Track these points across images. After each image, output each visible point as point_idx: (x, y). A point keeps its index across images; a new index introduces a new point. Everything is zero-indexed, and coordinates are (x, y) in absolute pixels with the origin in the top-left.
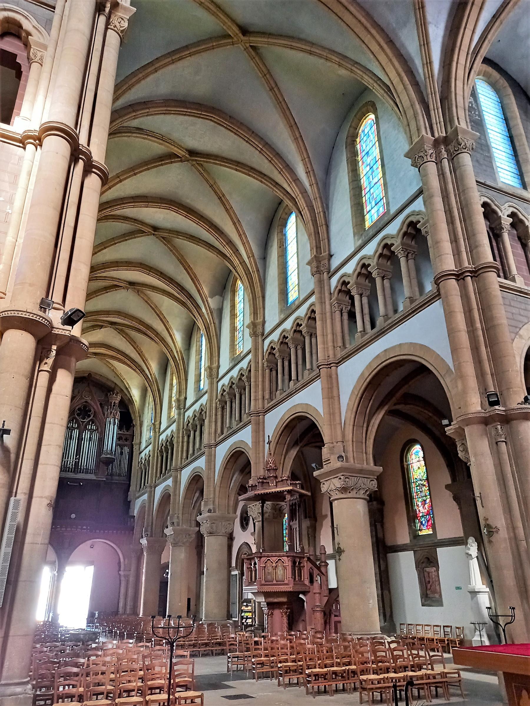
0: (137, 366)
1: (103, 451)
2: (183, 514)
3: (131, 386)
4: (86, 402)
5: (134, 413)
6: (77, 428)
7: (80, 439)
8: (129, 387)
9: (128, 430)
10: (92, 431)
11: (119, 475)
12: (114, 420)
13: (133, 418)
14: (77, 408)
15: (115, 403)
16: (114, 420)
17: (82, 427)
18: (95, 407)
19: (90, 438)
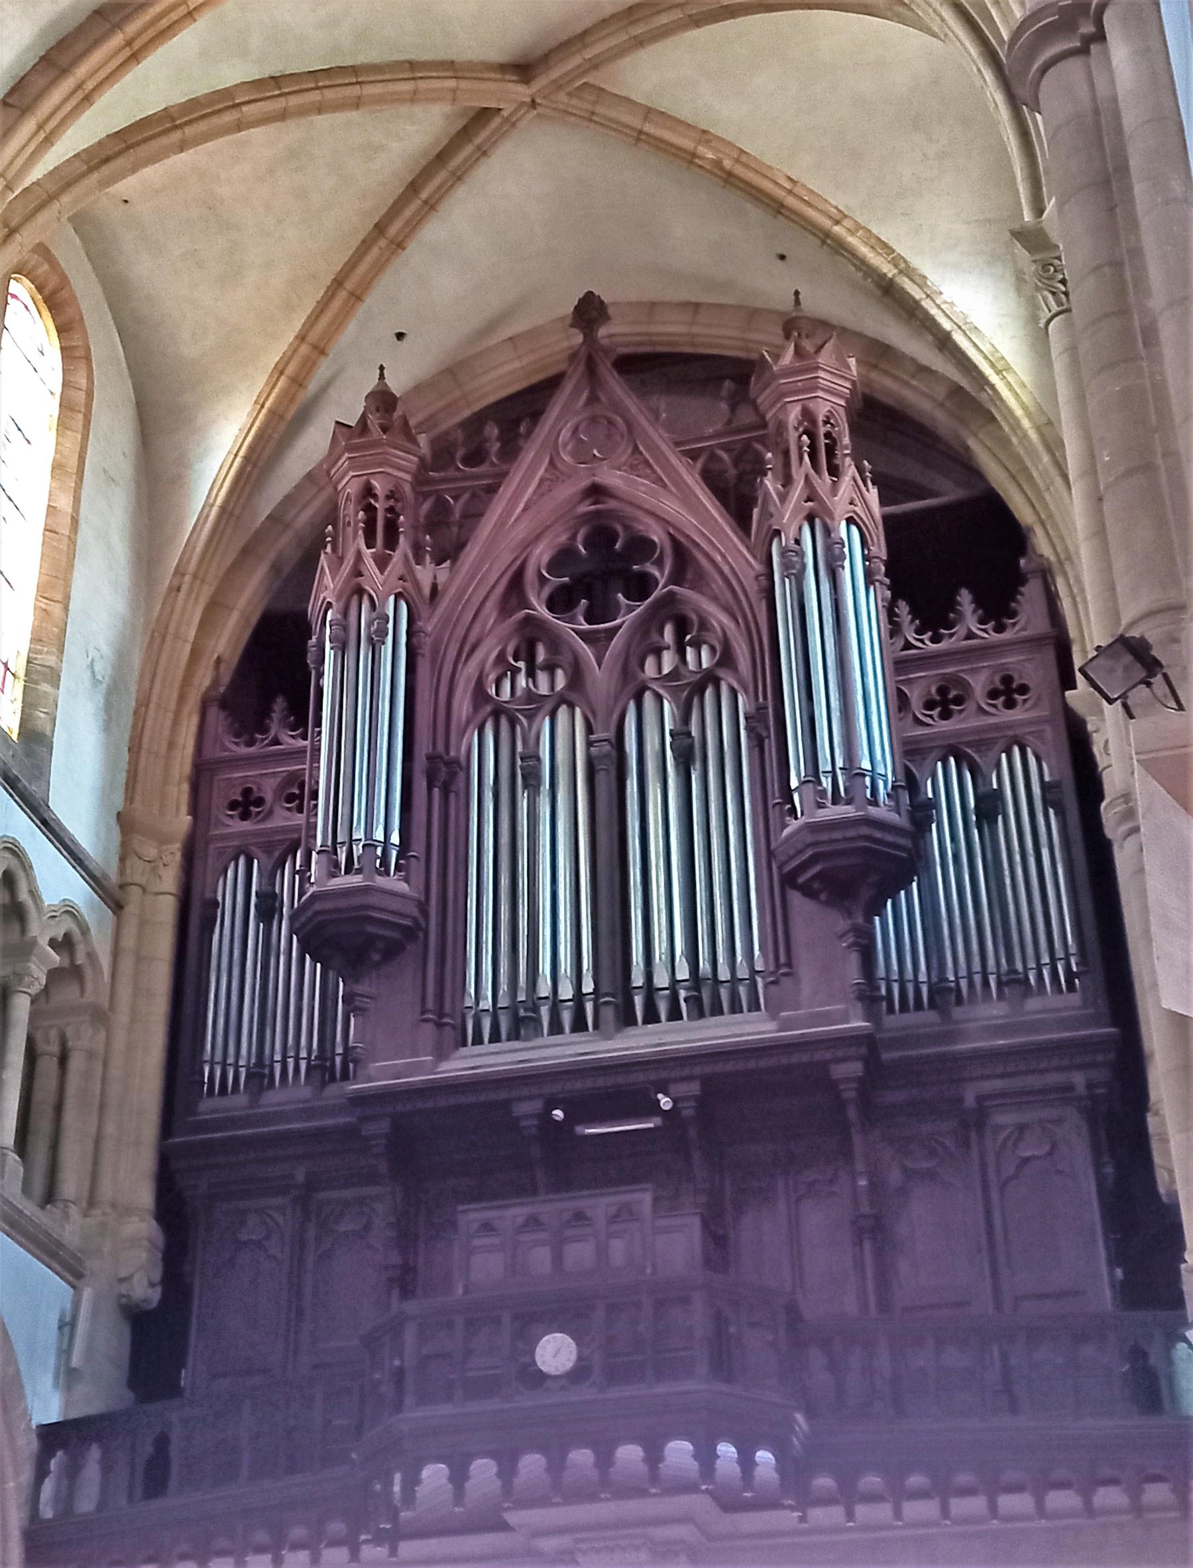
1: (787, 793)
3: (916, 262)
4: (596, 492)
5: (1020, 474)
7: (609, 771)
8: (908, 271)
9: (997, 609)
11: (1014, 983)
12: (827, 531)
13: (1024, 513)
14: (542, 554)
16: (827, 531)
17: (601, 676)
18: (671, 507)
19: (681, 734)
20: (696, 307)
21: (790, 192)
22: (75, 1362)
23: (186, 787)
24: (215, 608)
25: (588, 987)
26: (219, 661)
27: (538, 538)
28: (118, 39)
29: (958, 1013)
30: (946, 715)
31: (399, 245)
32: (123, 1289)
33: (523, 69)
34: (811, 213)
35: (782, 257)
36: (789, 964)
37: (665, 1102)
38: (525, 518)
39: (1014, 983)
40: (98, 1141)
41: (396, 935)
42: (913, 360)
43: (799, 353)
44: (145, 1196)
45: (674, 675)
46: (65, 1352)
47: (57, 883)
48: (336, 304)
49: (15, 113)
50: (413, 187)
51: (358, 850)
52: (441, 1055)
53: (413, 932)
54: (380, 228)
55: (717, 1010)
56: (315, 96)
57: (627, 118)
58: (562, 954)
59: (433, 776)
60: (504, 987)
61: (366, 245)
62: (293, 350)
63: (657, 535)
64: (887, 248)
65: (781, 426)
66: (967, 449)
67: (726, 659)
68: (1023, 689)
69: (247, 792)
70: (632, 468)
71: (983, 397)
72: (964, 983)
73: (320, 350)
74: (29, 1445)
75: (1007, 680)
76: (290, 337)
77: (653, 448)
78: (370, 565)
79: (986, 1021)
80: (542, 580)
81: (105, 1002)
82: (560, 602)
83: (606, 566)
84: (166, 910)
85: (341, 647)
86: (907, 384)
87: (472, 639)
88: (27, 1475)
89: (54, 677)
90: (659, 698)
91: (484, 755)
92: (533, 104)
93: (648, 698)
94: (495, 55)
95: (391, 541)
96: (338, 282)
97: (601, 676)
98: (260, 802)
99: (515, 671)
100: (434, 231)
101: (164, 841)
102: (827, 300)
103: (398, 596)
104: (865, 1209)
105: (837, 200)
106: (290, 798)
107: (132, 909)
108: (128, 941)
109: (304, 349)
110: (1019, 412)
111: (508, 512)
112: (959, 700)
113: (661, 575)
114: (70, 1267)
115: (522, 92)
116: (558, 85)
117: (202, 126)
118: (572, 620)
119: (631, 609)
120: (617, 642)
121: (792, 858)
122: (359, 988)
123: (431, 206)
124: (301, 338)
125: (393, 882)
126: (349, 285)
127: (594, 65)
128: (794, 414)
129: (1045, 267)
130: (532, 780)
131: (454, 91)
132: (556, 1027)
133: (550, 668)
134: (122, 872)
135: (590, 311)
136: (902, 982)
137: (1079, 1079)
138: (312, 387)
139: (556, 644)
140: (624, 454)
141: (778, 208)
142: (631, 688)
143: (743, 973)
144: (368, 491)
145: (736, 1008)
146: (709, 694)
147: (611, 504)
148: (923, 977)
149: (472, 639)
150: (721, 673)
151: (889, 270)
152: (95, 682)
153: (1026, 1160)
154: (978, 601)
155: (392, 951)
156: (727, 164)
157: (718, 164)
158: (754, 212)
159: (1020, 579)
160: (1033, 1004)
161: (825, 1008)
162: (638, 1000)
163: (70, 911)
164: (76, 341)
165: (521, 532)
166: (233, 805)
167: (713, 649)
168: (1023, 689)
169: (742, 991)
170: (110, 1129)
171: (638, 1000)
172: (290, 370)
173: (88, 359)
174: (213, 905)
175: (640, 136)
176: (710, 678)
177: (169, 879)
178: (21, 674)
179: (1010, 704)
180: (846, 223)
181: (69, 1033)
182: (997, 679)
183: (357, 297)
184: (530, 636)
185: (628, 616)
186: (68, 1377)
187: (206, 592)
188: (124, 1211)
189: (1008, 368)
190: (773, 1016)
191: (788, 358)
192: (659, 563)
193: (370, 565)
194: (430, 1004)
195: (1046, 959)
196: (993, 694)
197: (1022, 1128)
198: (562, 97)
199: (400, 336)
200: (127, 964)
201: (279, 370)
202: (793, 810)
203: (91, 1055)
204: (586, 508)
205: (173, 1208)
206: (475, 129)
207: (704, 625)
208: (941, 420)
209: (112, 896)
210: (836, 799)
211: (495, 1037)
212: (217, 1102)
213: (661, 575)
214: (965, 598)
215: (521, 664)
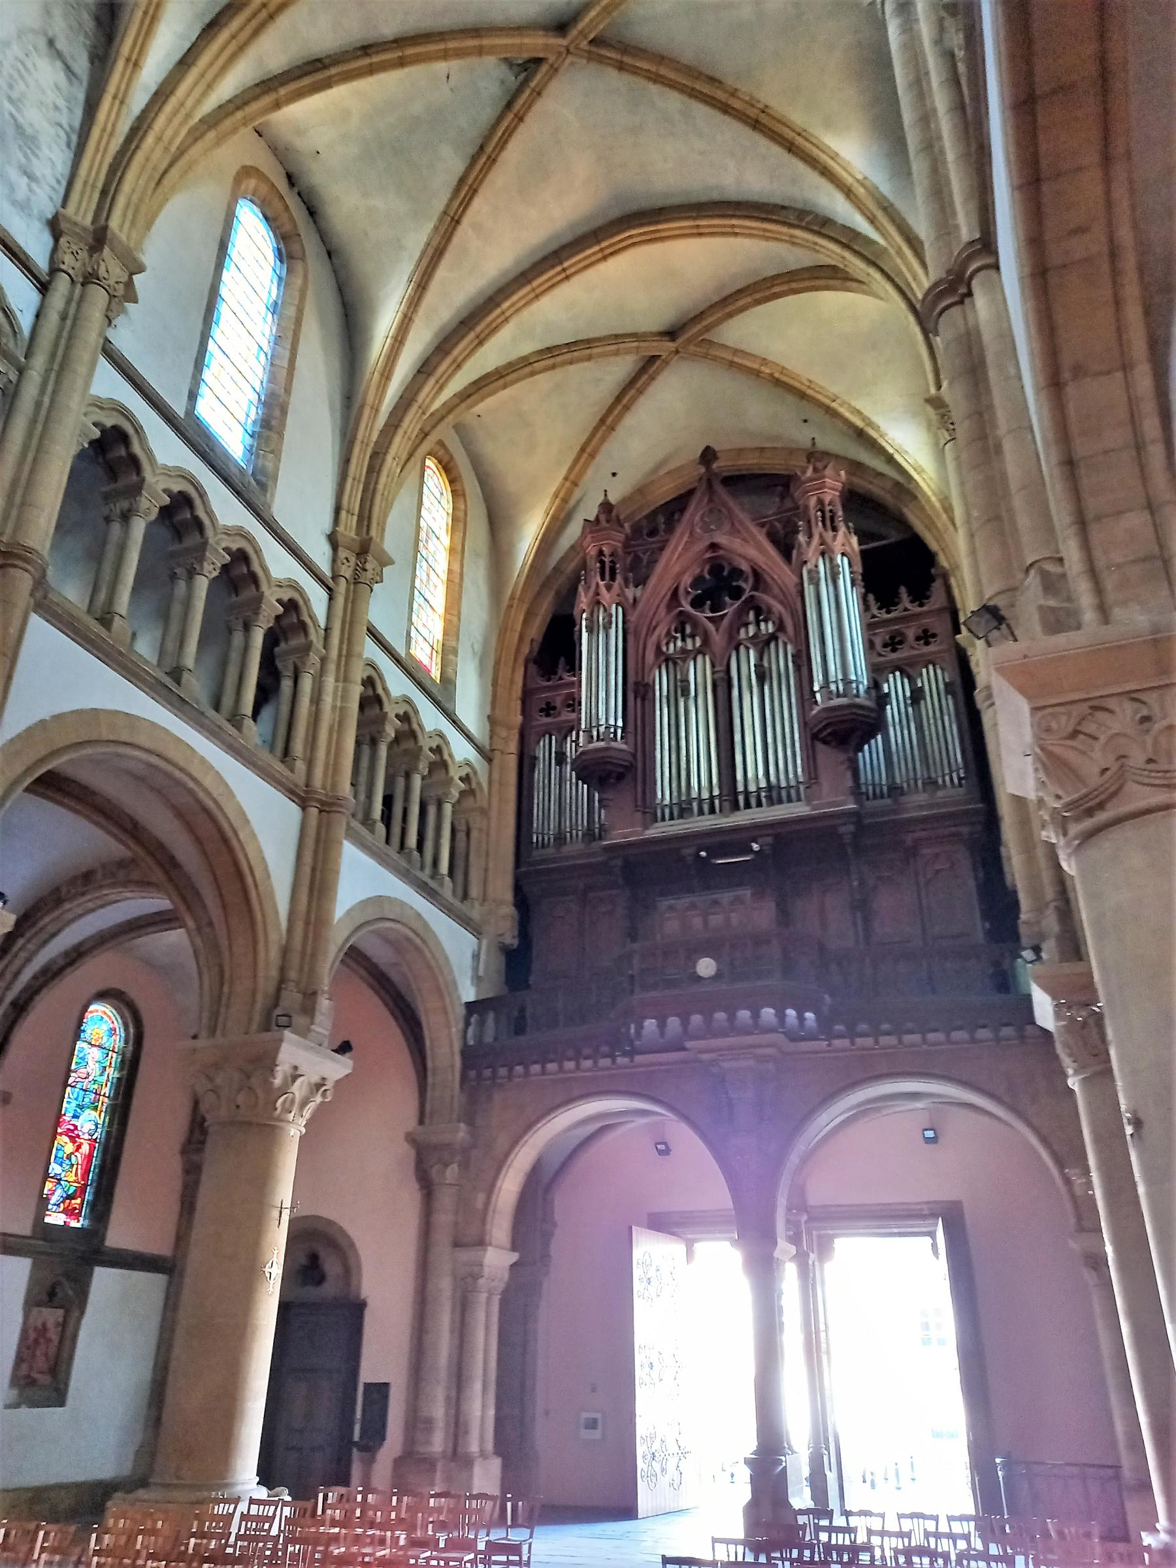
0: (792, 219)
2: (1082, 523)
4: (714, 546)
5: (931, 525)
6: (700, 651)
7: (723, 687)
8: (870, 423)
9: (920, 595)
10: (764, 644)
13: (933, 545)
14: (687, 580)
15: (820, 502)
16: (832, 560)
17: (718, 638)
18: (752, 552)
20: (762, 449)
21: (809, 387)
22: (481, 973)
23: (519, 702)
24: (529, 615)
25: (716, 792)
26: (532, 640)
27: (683, 573)
28: (472, 335)
29: (903, 799)
30: (894, 650)
31: (612, 428)
32: (500, 939)
33: (671, 334)
34: (819, 397)
35: (805, 421)
36: (816, 778)
37: (755, 847)
38: (678, 562)
39: (931, 783)
40: (486, 870)
41: (621, 770)
42: (874, 470)
43: (815, 470)
44: (509, 896)
45: (755, 636)
46: (476, 969)
47: (461, 751)
48: (582, 460)
49: (424, 376)
50: (618, 399)
51: (602, 729)
52: (646, 828)
53: (631, 768)
54: (602, 421)
55: (780, 802)
56: (568, 357)
57: (724, 355)
58: (702, 776)
59: (637, 693)
60: (675, 794)
61: (596, 430)
62: (562, 485)
63: (745, 567)
64: (859, 413)
65: (807, 507)
66: (902, 514)
67: (781, 627)
68: (934, 636)
69: (548, 704)
70: (730, 534)
71: (911, 486)
72: (905, 785)
73: (575, 484)
74: (461, 1011)
75: (925, 631)
76: (560, 478)
77: (741, 523)
78: (603, 590)
79: (917, 803)
80: (688, 593)
81: (485, 804)
82: (697, 603)
83: (720, 583)
84: (512, 761)
85: (590, 630)
86: (871, 483)
87: (654, 623)
88: (461, 1025)
89: (455, 652)
90: (747, 649)
91: (662, 682)
92: (677, 352)
93: (742, 649)
94: (655, 328)
95: (613, 578)
96: (583, 450)
97: (718, 638)
98: (554, 708)
99: (676, 638)
100: (629, 420)
101: (510, 728)
102: (829, 442)
103: (617, 604)
104: (858, 897)
105: (833, 389)
106: (569, 706)
107: (496, 762)
108: (496, 776)
109: (568, 484)
110: (929, 493)
111: (670, 559)
112: (901, 642)
113: (747, 586)
114: (477, 932)
115: (671, 346)
116: (689, 341)
117: (514, 376)
118: (703, 612)
119: (732, 605)
120: (726, 622)
121: (816, 726)
122: (605, 796)
123: (627, 408)
124: (566, 479)
125: (619, 744)
126: (589, 450)
127: (707, 329)
128: (813, 502)
129: (943, 416)
130: (685, 692)
131: (637, 348)
132: (701, 812)
133: (693, 636)
134: (491, 744)
135: (708, 455)
136: (874, 785)
137: (965, 830)
138: (572, 502)
139: (695, 624)
140: (727, 527)
141: (802, 396)
142: (734, 644)
143: (793, 783)
144: (601, 553)
145: (790, 800)
146: (772, 645)
147: (721, 552)
148: (884, 782)
149: (654, 623)
150: (780, 635)
151: (859, 423)
152: (474, 653)
153: (937, 872)
154: (910, 593)
155: (620, 777)
156: (777, 375)
157: (771, 375)
158: (790, 399)
159: (932, 579)
160: (940, 794)
161: (834, 799)
162: (741, 798)
163: (468, 764)
164: (458, 487)
165: (677, 569)
166: (541, 710)
167: (774, 623)
168: (934, 636)
169: (793, 792)
170: (491, 865)
171: (741, 798)
172: (561, 495)
173: (464, 495)
174: (535, 758)
175: (732, 364)
176: (774, 637)
177: (513, 747)
178: (440, 650)
179: (927, 643)
180: (838, 401)
181: (471, 822)
182: (920, 631)
183: (592, 456)
184: (682, 621)
185: (731, 608)
186: (477, 980)
187: (525, 607)
188: (502, 903)
189: (923, 471)
190: (809, 801)
191: (809, 473)
192: (746, 581)
193: (603, 590)
194: (639, 803)
195: (947, 771)
196: (918, 639)
197: (937, 855)
198: (692, 348)
199: (614, 474)
200: (496, 787)
201: (556, 496)
202: (816, 702)
203: (480, 830)
204: (708, 555)
205: (522, 901)
206: (648, 367)
207: (769, 611)
208: (889, 499)
209: (487, 755)
210: (838, 695)
211: (672, 818)
212: (541, 851)
213: (747, 586)
214: (903, 590)
215: (678, 635)
